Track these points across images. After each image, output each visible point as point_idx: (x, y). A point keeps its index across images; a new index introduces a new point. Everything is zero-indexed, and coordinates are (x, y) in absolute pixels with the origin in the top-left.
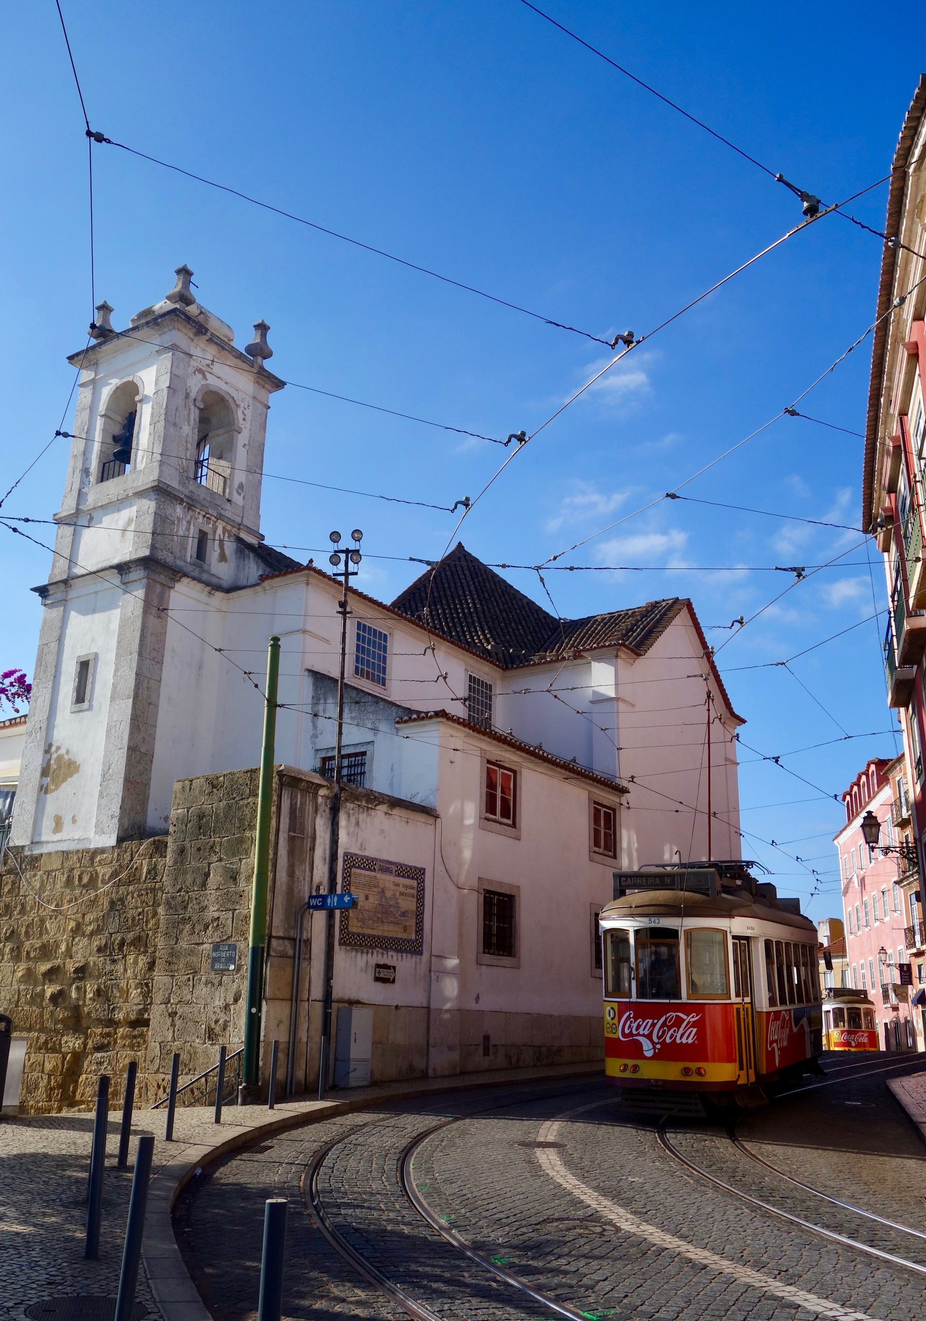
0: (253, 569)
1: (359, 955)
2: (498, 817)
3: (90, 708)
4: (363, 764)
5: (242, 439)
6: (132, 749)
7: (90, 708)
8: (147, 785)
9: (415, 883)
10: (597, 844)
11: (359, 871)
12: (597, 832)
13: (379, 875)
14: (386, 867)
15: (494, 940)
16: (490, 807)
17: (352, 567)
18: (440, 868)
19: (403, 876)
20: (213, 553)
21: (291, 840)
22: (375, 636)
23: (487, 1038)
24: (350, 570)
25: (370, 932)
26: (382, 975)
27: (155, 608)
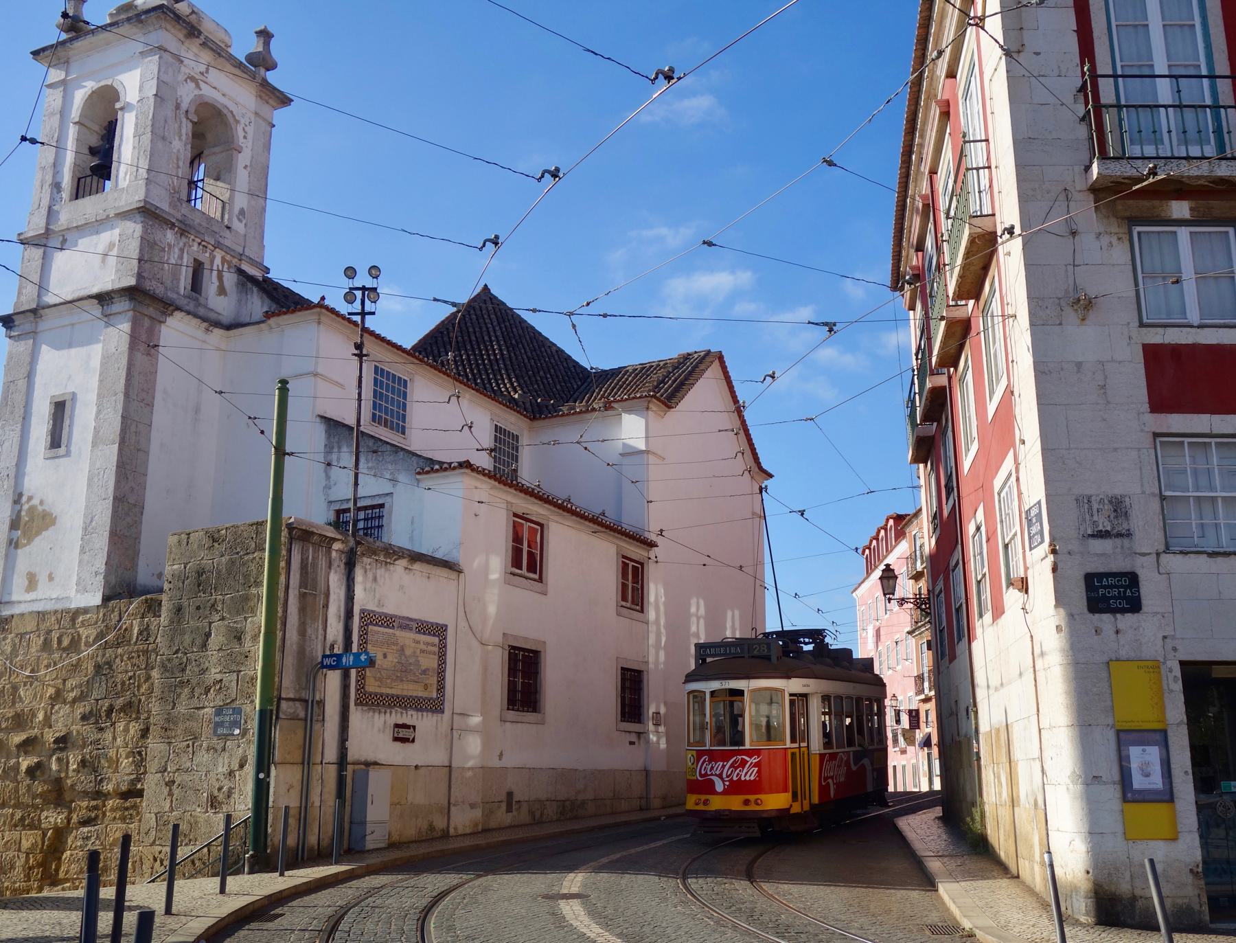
0: (257, 305)
1: (377, 715)
2: (524, 571)
3: (68, 454)
4: (380, 517)
5: (243, 159)
6: (119, 500)
7: (68, 454)
8: (137, 539)
9: (436, 640)
10: (624, 598)
11: (376, 628)
12: (624, 586)
13: (398, 633)
14: (405, 624)
15: (519, 696)
16: (517, 563)
17: (369, 306)
18: (463, 624)
19: (424, 633)
20: (210, 285)
21: (303, 596)
22: (394, 382)
24: (367, 309)
25: (389, 691)
26: (401, 735)
27: (144, 344)
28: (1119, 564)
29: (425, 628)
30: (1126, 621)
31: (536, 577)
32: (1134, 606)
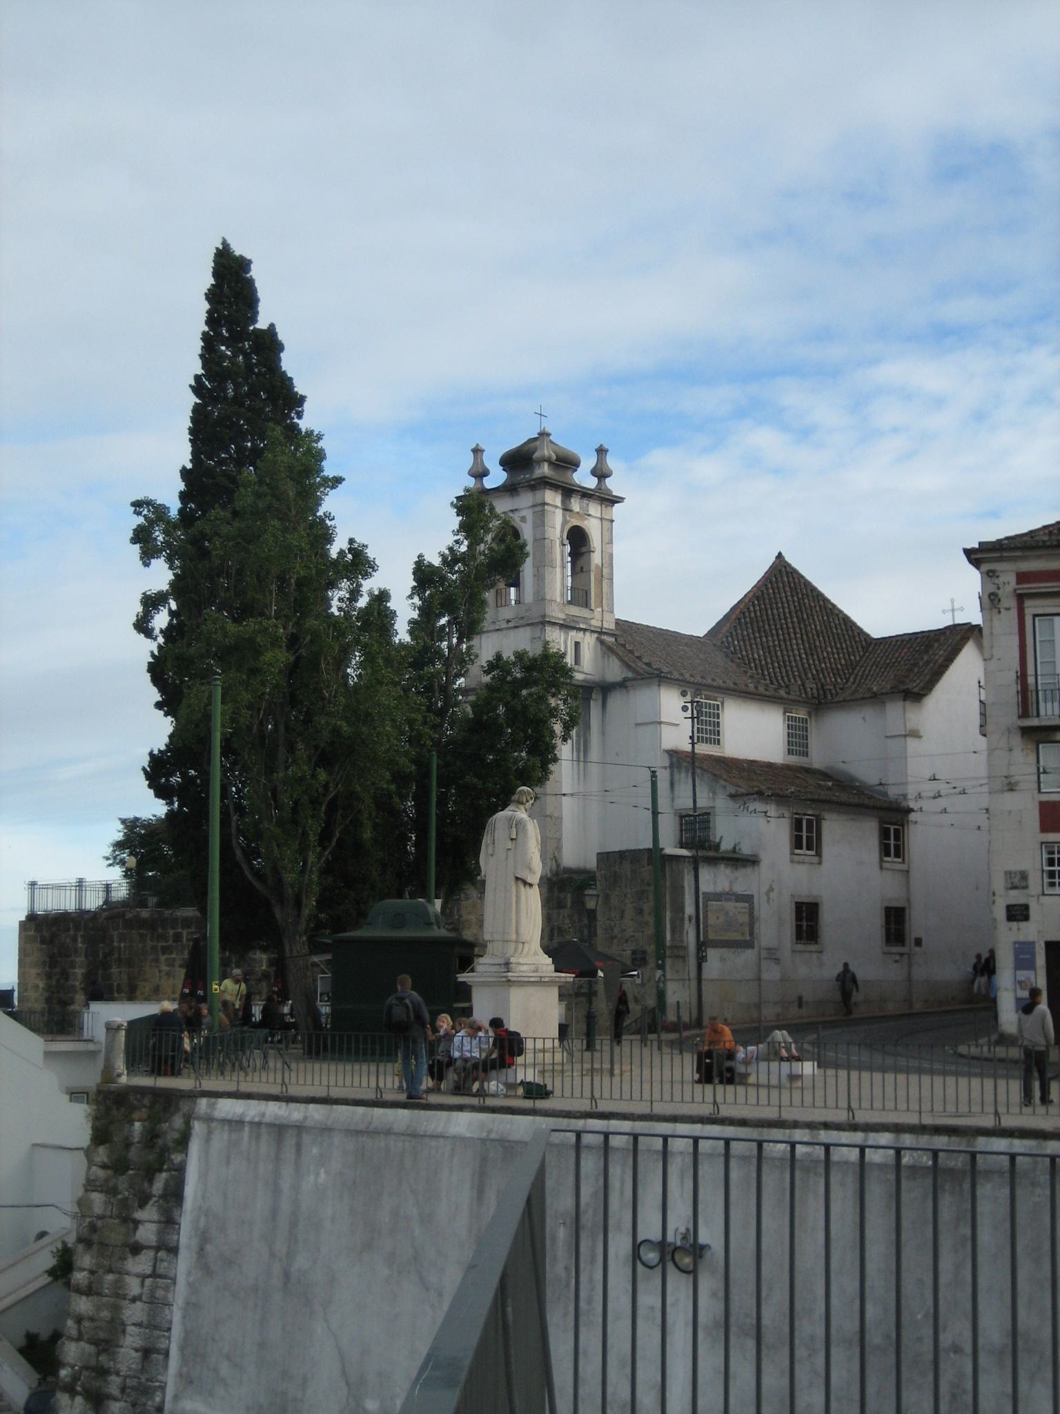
16: (797, 843)
23: (800, 999)
28: (1022, 901)
30: (1023, 925)
31: (813, 853)
32: (1026, 918)
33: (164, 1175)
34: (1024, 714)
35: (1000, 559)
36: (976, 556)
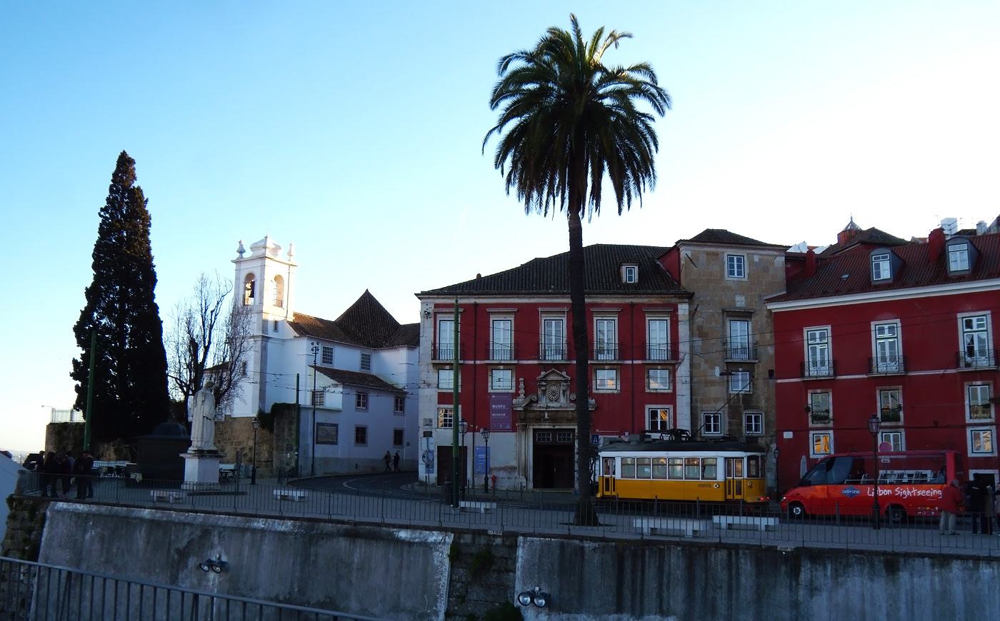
6: (260, 390)
8: (265, 398)
16: (359, 405)
23: (356, 465)
29: (332, 425)
33: (35, 532)
34: (434, 358)
35: (429, 298)
36: (422, 296)
